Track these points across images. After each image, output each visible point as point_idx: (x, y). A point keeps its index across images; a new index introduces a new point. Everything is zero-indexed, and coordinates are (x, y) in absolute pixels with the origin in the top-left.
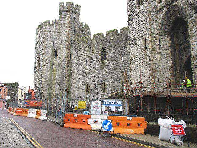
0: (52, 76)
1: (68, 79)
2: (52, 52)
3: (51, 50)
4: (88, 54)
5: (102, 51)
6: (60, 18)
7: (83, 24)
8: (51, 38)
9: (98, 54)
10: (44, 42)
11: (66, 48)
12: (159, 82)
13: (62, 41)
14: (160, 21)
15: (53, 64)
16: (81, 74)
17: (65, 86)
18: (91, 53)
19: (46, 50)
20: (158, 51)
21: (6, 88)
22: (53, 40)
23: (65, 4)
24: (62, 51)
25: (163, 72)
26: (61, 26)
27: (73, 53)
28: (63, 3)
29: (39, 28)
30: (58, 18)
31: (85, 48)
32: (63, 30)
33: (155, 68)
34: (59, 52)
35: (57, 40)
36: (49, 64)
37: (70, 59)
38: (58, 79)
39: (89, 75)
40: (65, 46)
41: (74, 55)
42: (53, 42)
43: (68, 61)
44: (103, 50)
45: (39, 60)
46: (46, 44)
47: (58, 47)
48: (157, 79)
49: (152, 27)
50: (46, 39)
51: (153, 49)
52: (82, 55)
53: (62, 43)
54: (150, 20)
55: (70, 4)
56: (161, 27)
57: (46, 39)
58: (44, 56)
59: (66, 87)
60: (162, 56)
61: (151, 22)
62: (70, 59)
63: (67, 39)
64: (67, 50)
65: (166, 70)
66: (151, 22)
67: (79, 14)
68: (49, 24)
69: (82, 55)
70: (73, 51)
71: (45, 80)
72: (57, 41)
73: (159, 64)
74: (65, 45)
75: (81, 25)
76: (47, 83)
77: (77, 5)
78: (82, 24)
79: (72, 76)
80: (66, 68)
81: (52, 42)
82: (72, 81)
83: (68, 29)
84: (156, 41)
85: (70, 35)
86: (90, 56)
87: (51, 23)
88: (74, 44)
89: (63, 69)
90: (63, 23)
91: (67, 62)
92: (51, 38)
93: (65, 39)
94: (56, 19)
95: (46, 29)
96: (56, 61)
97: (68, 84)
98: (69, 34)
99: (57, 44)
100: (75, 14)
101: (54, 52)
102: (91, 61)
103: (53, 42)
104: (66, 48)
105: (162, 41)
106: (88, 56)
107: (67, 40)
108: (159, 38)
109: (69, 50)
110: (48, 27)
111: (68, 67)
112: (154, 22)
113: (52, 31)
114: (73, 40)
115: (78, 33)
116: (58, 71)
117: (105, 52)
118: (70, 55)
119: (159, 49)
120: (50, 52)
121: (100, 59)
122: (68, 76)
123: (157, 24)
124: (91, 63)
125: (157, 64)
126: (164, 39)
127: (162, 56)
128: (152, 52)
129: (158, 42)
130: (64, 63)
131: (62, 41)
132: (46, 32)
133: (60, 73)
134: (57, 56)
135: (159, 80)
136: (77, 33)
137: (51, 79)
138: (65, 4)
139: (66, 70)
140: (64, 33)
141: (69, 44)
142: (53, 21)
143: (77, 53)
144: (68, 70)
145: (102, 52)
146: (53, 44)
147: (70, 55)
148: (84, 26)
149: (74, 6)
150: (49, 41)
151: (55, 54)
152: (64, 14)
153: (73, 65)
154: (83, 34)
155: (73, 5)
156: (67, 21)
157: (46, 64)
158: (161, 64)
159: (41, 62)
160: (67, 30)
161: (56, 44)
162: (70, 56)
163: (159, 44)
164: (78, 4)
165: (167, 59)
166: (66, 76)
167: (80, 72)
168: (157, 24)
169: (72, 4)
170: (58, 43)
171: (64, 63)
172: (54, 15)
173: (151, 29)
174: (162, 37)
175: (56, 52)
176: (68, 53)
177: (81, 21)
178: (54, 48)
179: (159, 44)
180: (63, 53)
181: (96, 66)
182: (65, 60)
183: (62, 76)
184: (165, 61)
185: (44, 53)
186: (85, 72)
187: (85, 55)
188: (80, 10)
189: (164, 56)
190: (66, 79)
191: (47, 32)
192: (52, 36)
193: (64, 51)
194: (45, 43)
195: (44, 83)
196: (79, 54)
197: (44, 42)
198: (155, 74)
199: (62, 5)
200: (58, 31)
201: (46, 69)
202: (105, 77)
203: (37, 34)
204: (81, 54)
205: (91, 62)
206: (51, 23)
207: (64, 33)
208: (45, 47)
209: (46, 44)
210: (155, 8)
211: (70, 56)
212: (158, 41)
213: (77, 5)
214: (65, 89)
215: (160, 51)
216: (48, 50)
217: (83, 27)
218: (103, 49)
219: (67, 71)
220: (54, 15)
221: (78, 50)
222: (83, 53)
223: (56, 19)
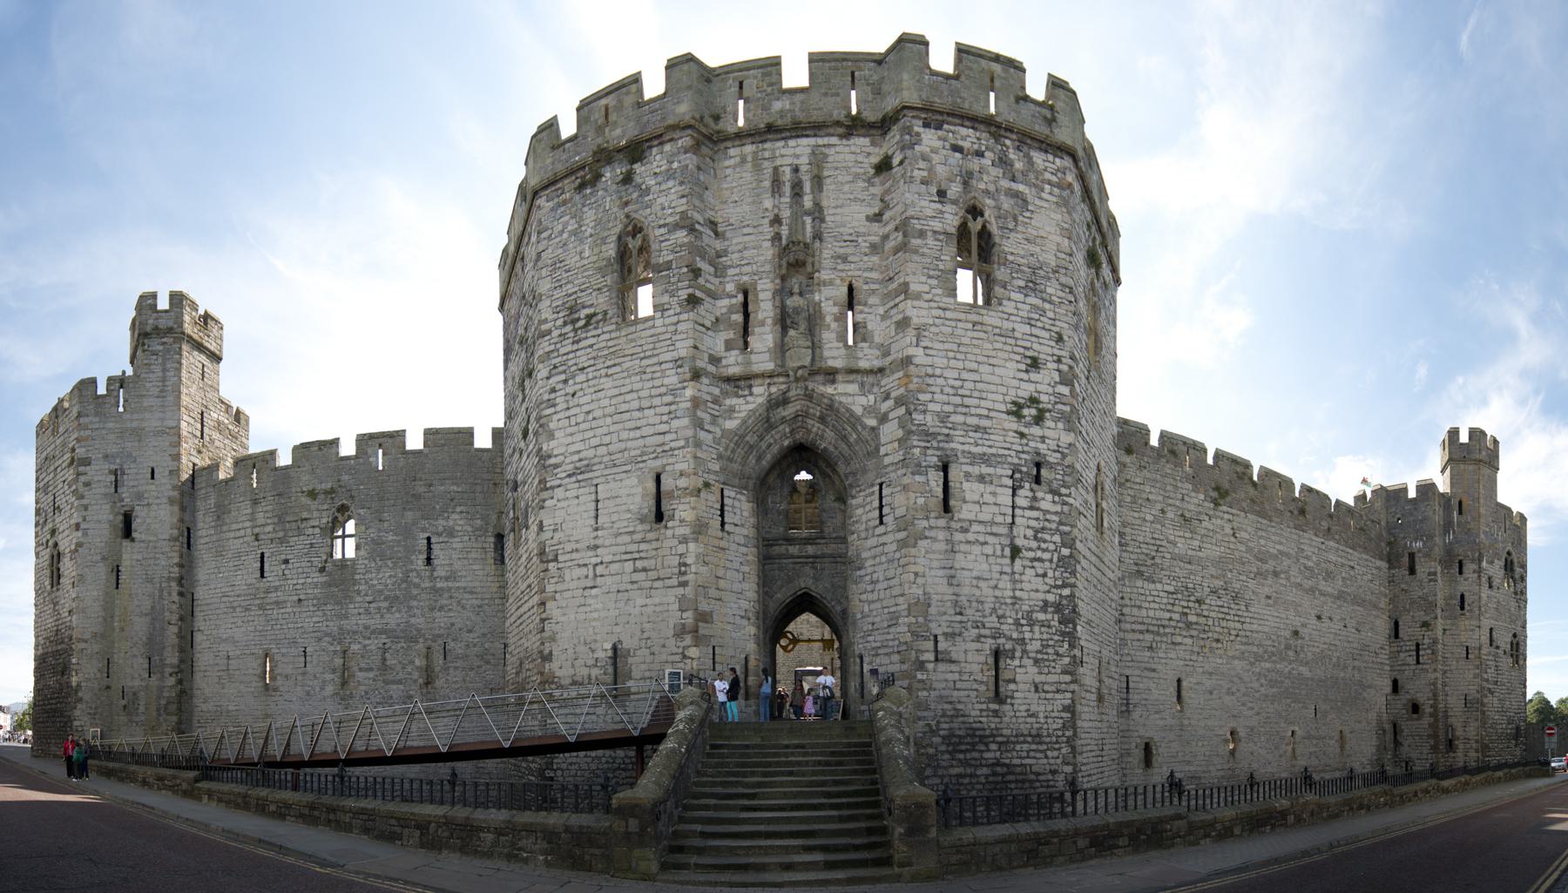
8: (106, 456)
10: (78, 474)
11: (171, 501)
17: (172, 658)
22: (113, 467)
27: (200, 525)
32: (155, 424)
36: (102, 571)
38: (140, 626)
41: (204, 530)
43: (181, 557)
47: (140, 496)
50: (86, 462)
57: (86, 462)
58: (80, 534)
59: (175, 661)
64: (176, 508)
72: (130, 469)
76: (96, 648)
80: (173, 584)
82: (198, 637)
87: (102, 390)
89: (161, 590)
91: (176, 560)
92: (106, 456)
96: (130, 555)
97: (182, 650)
101: (121, 518)
107: (172, 465)
109: (183, 509)
111: (180, 581)
113: (111, 425)
116: (138, 594)
120: (103, 517)
122: (181, 619)
130: (167, 562)
133: (147, 604)
134: (134, 535)
137: (113, 629)
139: (175, 594)
142: (110, 380)
144: (181, 594)
150: (99, 473)
151: (127, 528)
161: (128, 480)
162: (187, 538)
166: (175, 618)
170: (135, 478)
180: (157, 520)
183: (154, 615)
190: (175, 629)
191: (88, 432)
194: (82, 478)
195: (83, 645)
197: (78, 474)
199: (146, 302)
200: (135, 424)
201: (84, 592)
204: (234, 526)
206: (102, 390)
208: (82, 497)
209: (87, 484)
211: (187, 538)
214: (169, 670)
219: (176, 598)
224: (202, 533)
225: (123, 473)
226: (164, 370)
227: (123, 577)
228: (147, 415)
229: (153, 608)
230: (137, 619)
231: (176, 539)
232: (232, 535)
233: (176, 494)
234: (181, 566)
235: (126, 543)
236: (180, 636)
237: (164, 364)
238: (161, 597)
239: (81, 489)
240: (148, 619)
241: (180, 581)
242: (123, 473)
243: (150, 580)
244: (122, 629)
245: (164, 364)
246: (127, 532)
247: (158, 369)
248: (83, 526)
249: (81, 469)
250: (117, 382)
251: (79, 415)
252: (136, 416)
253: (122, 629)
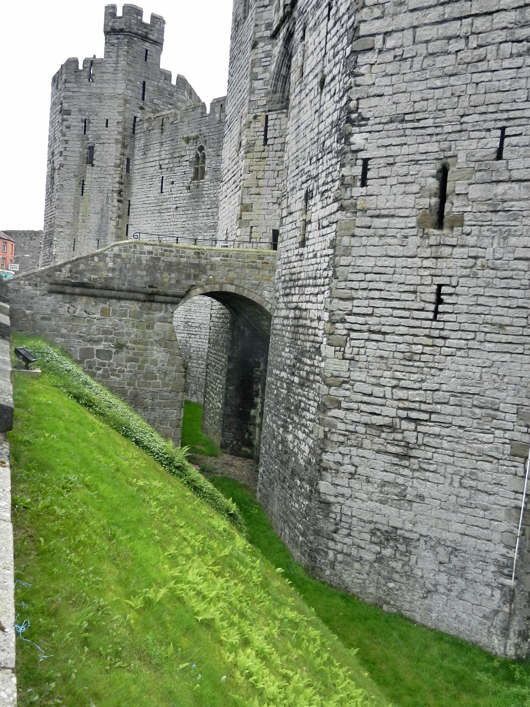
0: (81, 214)
1: (118, 222)
2: (81, 150)
3: (79, 143)
4: (166, 161)
5: (198, 154)
6: (107, 53)
7: (170, 76)
8: (80, 110)
9: (188, 163)
10: (63, 120)
11: (117, 141)
12: (251, 238)
13: (107, 120)
14: (273, 67)
15: (83, 181)
16: (150, 212)
18: (176, 157)
19: (66, 142)
20: (259, 155)
21: (9, 243)
22: (84, 118)
23: (119, 13)
24: (106, 149)
25: (263, 212)
26: (106, 77)
27: (136, 157)
28: (114, 7)
29: (55, 80)
30: (100, 54)
31: (161, 144)
32: (111, 91)
33: (247, 201)
34: (98, 148)
35: (95, 117)
36: (74, 183)
37: (128, 170)
39: (165, 216)
40: (114, 137)
42: (85, 123)
43: (121, 177)
44: (198, 152)
45: (53, 169)
46: (68, 127)
47: (98, 138)
48: (249, 229)
49: (258, 84)
51: (251, 146)
52: (153, 164)
53: (107, 126)
54: (253, 65)
55: (133, 11)
56: (275, 85)
60: (267, 168)
61: (255, 70)
62: (128, 170)
63: (121, 117)
64: (120, 146)
65: (271, 206)
66: (255, 70)
67: (159, 43)
68: (77, 70)
69: (153, 164)
70: (136, 152)
71: (63, 224)
73: (257, 190)
74: (114, 132)
75: (165, 79)
76: (68, 232)
77: (155, 18)
78: (167, 76)
79: (130, 217)
80: (115, 195)
81: (82, 121)
83: (124, 86)
84: (259, 125)
85: (128, 105)
86: (171, 165)
88: (139, 131)
89: (108, 198)
90: (111, 70)
91: (118, 179)
92: (80, 110)
93: (115, 117)
94: (95, 56)
95: (67, 85)
96: (91, 174)
98: (126, 101)
99: (94, 129)
100: (147, 44)
102: (171, 180)
103: (85, 123)
104: (117, 141)
105: (274, 125)
106: (167, 166)
107: (120, 118)
108: (267, 116)
109: (124, 146)
110: (72, 78)
111: (120, 192)
112: (260, 70)
113: (84, 90)
114: (137, 119)
115: (155, 101)
117: (204, 157)
118: (128, 160)
119: (262, 148)
120: (76, 148)
121: (192, 175)
122: (119, 217)
123: (267, 75)
124: (171, 186)
125: (254, 190)
126: (277, 122)
127: (267, 168)
128: (246, 157)
129: (263, 129)
130: (112, 181)
131: (107, 120)
132: (67, 93)
133: (98, 208)
134: (94, 162)
135: (251, 233)
136: (152, 101)
138: (119, 13)
139: (115, 201)
140: (112, 97)
141: (125, 129)
142: (85, 61)
143: (145, 156)
144: (119, 201)
145: (197, 157)
146: (85, 127)
147: (128, 160)
148: (174, 82)
149: (146, 19)
150: (75, 120)
152: (116, 41)
153: (135, 188)
154: (170, 106)
155: (141, 15)
156: (123, 63)
157: (65, 180)
158: (263, 191)
159: (56, 176)
160: (120, 91)
161: (92, 127)
162: (127, 165)
163: (265, 135)
164: (158, 13)
165: (278, 176)
166: (114, 216)
167: (148, 209)
168: (267, 75)
169: (139, 12)
171: (110, 181)
172: (91, 44)
173: (252, 91)
174: (275, 116)
175: (91, 149)
176: (123, 154)
177: (164, 64)
178: (88, 140)
179: (265, 135)
180: (109, 154)
181: (182, 195)
182: (113, 172)
184: (272, 182)
185: (63, 150)
186: (158, 208)
187: (161, 162)
188: (161, 31)
189: (271, 167)
190: (114, 223)
191: (70, 93)
192: (84, 106)
193: (111, 149)
194: (65, 123)
195: (60, 230)
196: (147, 160)
197: (63, 120)
198: (246, 216)
200: (98, 91)
202: (198, 223)
203: (52, 96)
204: (151, 159)
205: (173, 183)
207: (112, 97)
209: (68, 127)
210: (269, 26)
211: (127, 165)
212: (262, 126)
213: (155, 18)
215: (264, 154)
216: (71, 143)
217: (172, 86)
218: (201, 149)
219: (116, 203)
220: (91, 44)
221: (146, 150)
222: (157, 158)
223: (95, 56)
224: (136, 162)
225: (89, 122)
226: (118, 56)
227: (86, 188)
228: (106, 85)
229: (102, 209)
230: (92, 215)
231: (118, 166)
232: (149, 164)
233: (119, 137)
234: (121, 183)
235: (89, 167)
236: (117, 227)
237: (117, 52)
238: (107, 203)
239: (65, 130)
240: (99, 216)
241: (120, 192)
242: (89, 122)
243: (101, 192)
244: (84, 222)
245: (117, 52)
246: (90, 161)
247: (113, 55)
248: (64, 154)
249: (65, 117)
250: (91, 63)
251: (66, 82)
252: (99, 86)
253: (84, 222)
